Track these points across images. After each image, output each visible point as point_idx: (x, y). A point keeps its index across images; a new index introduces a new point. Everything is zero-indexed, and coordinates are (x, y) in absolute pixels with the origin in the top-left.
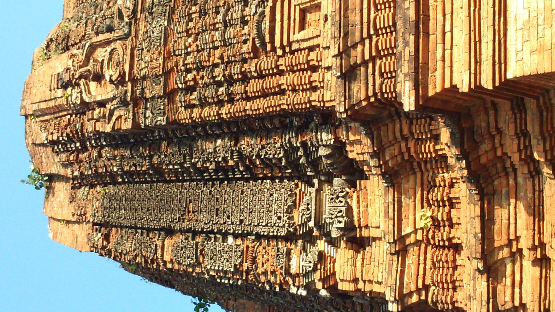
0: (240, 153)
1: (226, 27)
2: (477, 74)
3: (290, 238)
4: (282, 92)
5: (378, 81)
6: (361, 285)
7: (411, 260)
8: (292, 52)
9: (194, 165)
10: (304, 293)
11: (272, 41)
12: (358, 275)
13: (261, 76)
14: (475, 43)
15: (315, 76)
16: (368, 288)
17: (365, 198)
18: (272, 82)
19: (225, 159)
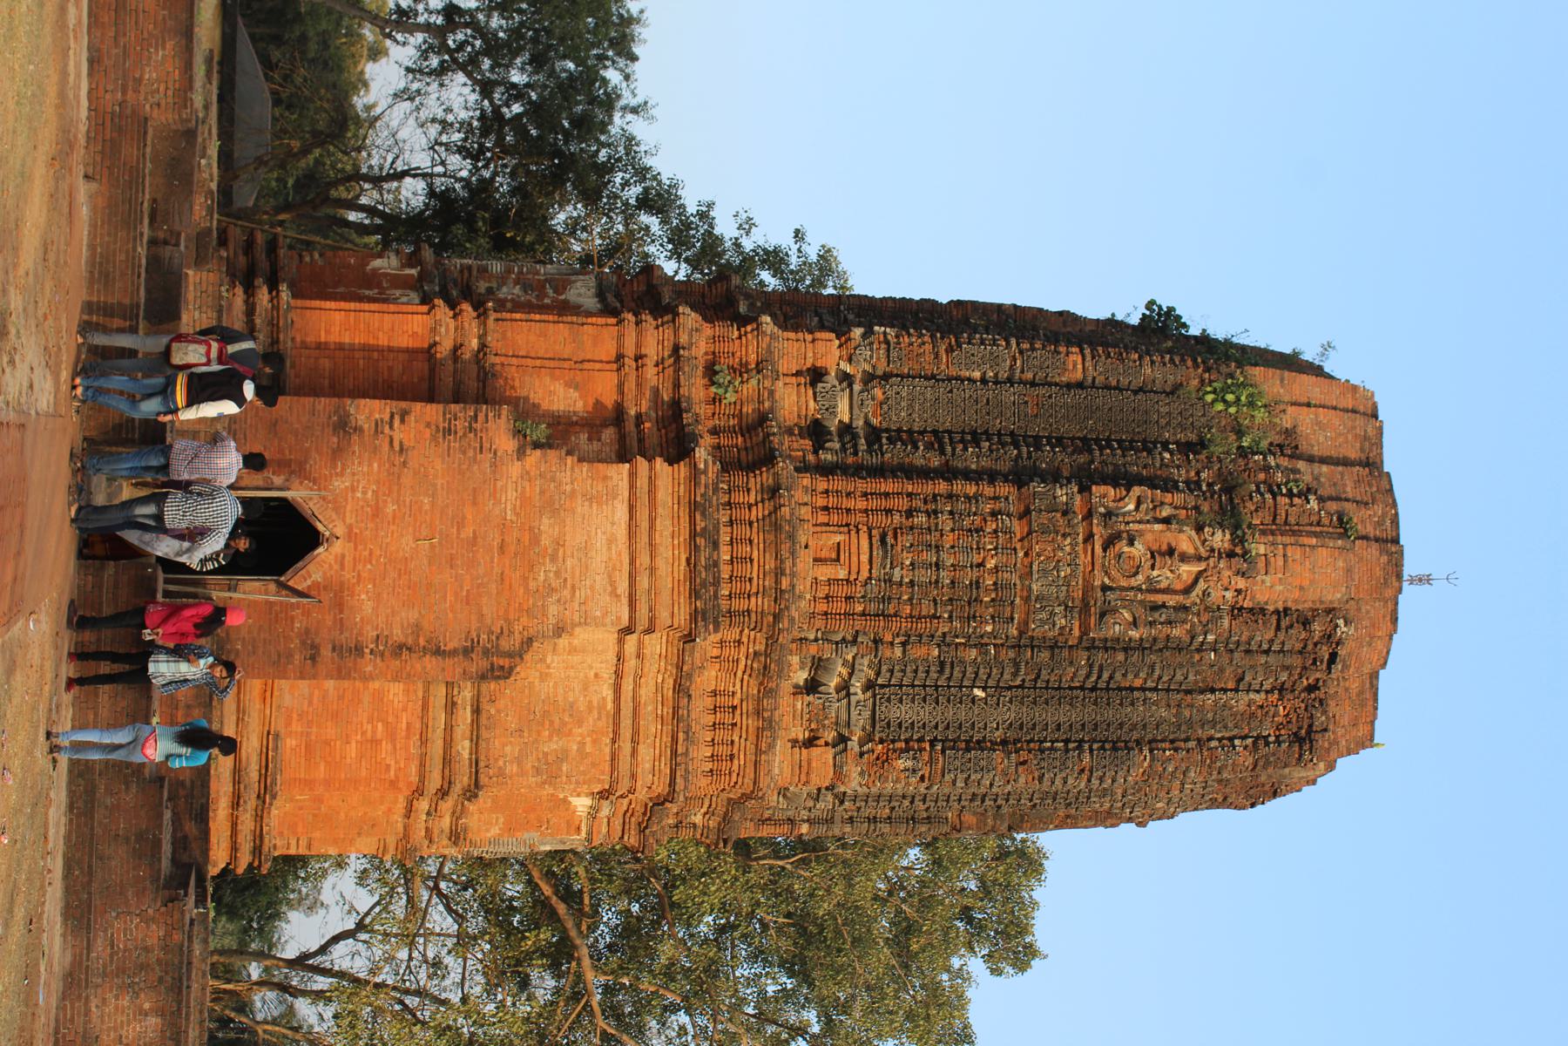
0: (942, 452)
1: (937, 565)
2: (651, 469)
3: (886, 377)
4: (865, 495)
5: (752, 484)
6: (809, 337)
7: (753, 357)
8: (847, 525)
9: (1017, 447)
10: (876, 328)
11: (870, 537)
12: (810, 346)
13: (888, 511)
14: (652, 491)
15: (821, 502)
16: (800, 335)
17: (799, 409)
18: (874, 503)
19: (965, 449)
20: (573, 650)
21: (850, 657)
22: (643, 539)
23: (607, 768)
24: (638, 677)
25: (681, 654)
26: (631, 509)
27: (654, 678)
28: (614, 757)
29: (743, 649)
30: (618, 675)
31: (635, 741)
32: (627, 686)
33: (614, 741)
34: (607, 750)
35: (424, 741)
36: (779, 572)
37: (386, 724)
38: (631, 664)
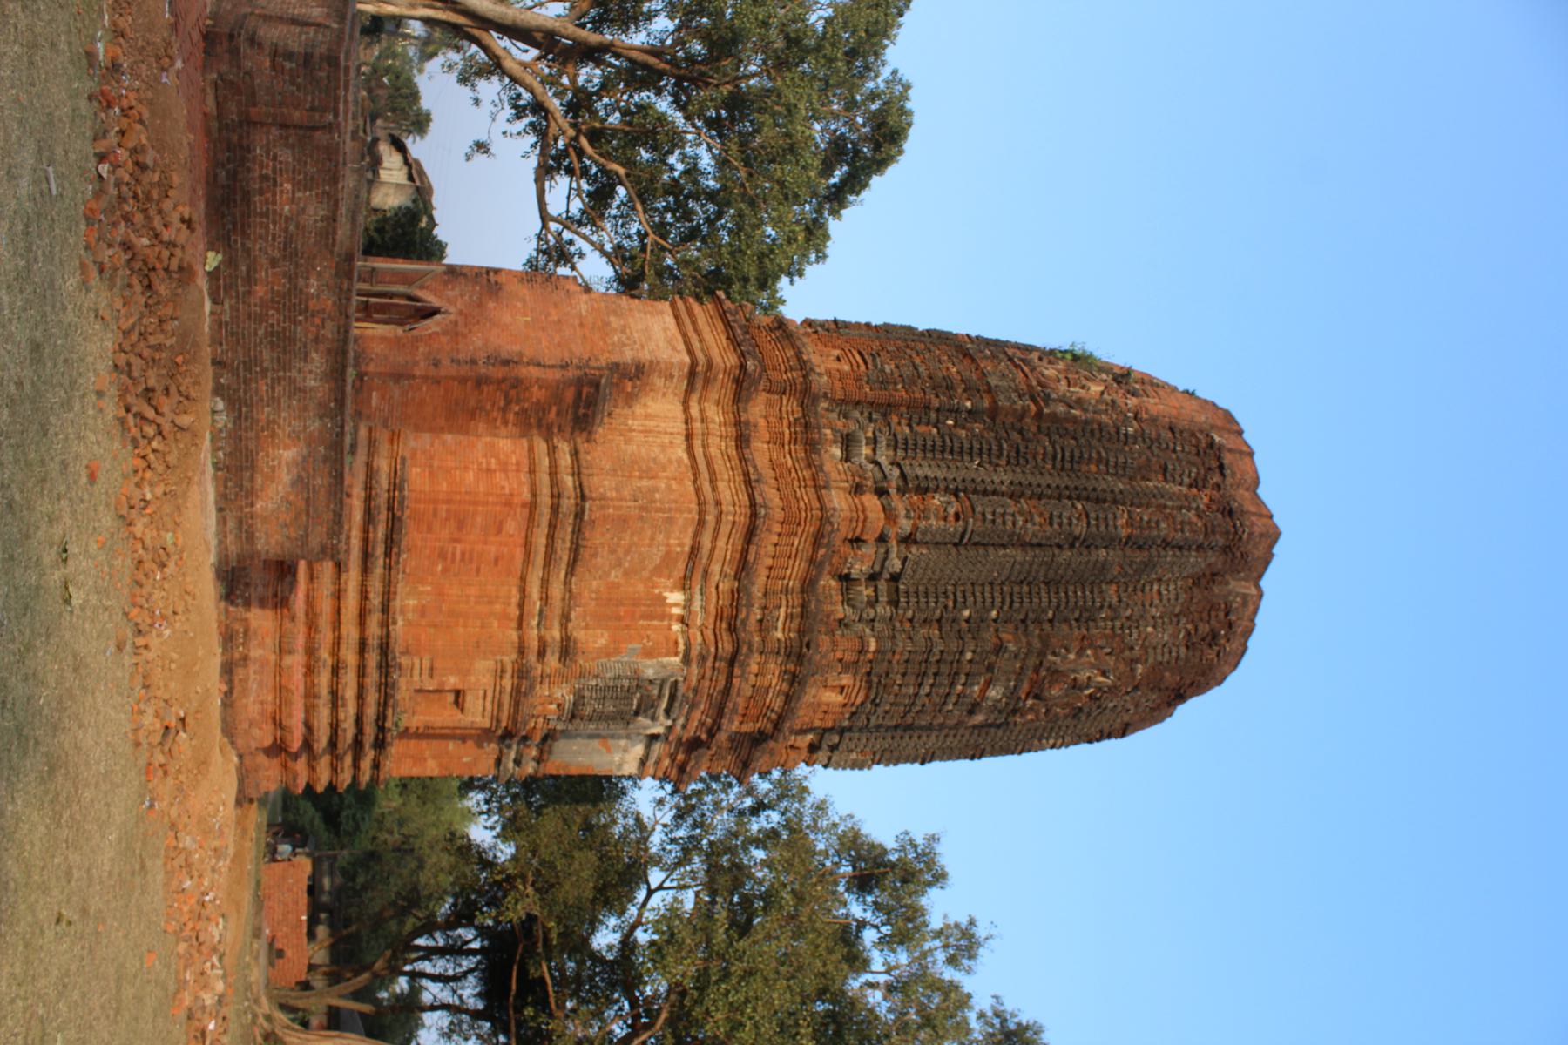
20: (647, 417)
21: (870, 434)
22: (689, 327)
23: (694, 498)
24: (706, 434)
25: (737, 414)
26: (677, 317)
27: (719, 446)
28: (698, 491)
29: (785, 422)
30: (689, 437)
31: (713, 481)
32: (697, 443)
33: (695, 482)
34: (691, 488)
35: (532, 471)
36: (799, 354)
37: (497, 458)
38: (697, 425)
